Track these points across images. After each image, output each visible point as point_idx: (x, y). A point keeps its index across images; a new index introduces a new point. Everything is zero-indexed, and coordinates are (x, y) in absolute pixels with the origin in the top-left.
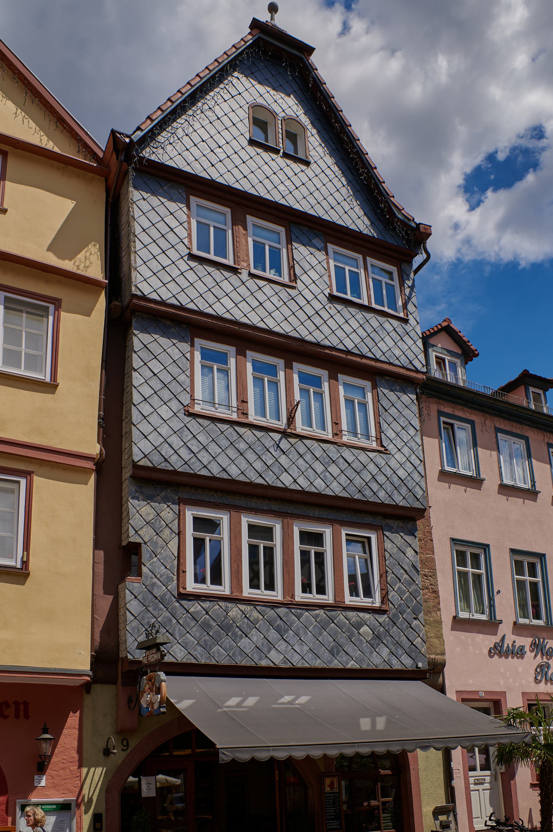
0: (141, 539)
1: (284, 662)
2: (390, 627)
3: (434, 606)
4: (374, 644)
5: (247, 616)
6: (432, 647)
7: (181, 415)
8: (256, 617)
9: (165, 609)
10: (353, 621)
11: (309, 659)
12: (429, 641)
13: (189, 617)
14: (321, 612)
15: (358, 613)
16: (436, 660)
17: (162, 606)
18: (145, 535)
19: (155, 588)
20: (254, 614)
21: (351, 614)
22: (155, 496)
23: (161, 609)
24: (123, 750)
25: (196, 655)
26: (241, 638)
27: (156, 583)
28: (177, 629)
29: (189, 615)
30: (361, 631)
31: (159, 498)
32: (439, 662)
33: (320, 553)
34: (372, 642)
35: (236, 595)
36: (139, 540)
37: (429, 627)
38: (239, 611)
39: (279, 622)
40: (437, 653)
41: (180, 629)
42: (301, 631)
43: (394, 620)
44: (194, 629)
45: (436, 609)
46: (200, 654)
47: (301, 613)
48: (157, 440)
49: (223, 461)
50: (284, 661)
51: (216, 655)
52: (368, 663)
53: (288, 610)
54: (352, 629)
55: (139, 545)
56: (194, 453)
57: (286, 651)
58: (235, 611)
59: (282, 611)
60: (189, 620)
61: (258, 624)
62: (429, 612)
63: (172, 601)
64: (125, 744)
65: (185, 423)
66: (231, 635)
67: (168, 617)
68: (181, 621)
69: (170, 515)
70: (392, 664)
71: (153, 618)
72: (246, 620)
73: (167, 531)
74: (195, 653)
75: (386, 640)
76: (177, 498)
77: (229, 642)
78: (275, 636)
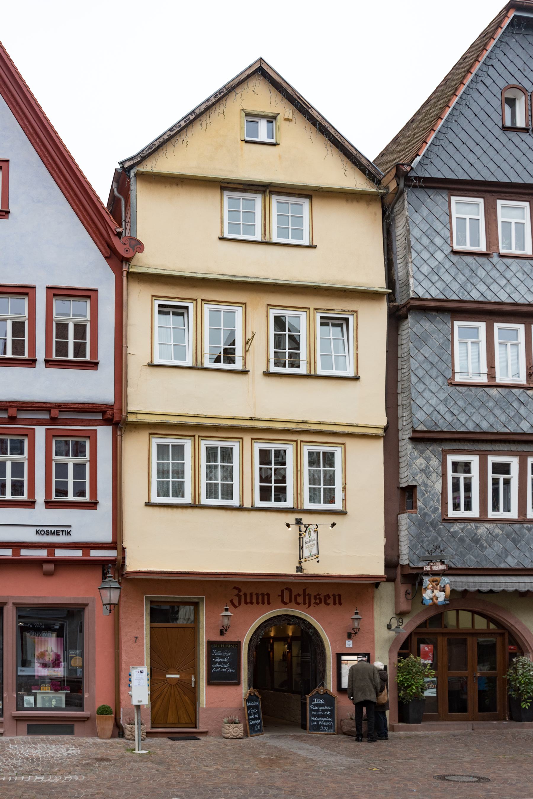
0: (416, 483)
1: (518, 565)
5: (491, 532)
7: (445, 387)
8: (497, 532)
9: (433, 531)
17: (431, 529)
18: (419, 480)
19: (427, 516)
22: (425, 450)
23: (431, 531)
25: (455, 561)
26: (486, 548)
27: (427, 513)
28: (442, 544)
29: (450, 534)
31: (428, 451)
35: (483, 518)
36: (414, 483)
38: (485, 529)
39: (514, 535)
41: (443, 544)
44: (453, 544)
48: (428, 409)
49: (476, 418)
50: (518, 564)
53: (521, 526)
55: (415, 487)
56: (455, 415)
57: (519, 556)
58: (482, 529)
59: (517, 526)
60: (449, 537)
61: (499, 538)
65: (449, 393)
66: (480, 546)
67: (435, 536)
68: (444, 539)
69: (436, 463)
72: (490, 536)
73: (434, 475)
76: (441, 449)
77: (478, 552)
78: (511, 546)
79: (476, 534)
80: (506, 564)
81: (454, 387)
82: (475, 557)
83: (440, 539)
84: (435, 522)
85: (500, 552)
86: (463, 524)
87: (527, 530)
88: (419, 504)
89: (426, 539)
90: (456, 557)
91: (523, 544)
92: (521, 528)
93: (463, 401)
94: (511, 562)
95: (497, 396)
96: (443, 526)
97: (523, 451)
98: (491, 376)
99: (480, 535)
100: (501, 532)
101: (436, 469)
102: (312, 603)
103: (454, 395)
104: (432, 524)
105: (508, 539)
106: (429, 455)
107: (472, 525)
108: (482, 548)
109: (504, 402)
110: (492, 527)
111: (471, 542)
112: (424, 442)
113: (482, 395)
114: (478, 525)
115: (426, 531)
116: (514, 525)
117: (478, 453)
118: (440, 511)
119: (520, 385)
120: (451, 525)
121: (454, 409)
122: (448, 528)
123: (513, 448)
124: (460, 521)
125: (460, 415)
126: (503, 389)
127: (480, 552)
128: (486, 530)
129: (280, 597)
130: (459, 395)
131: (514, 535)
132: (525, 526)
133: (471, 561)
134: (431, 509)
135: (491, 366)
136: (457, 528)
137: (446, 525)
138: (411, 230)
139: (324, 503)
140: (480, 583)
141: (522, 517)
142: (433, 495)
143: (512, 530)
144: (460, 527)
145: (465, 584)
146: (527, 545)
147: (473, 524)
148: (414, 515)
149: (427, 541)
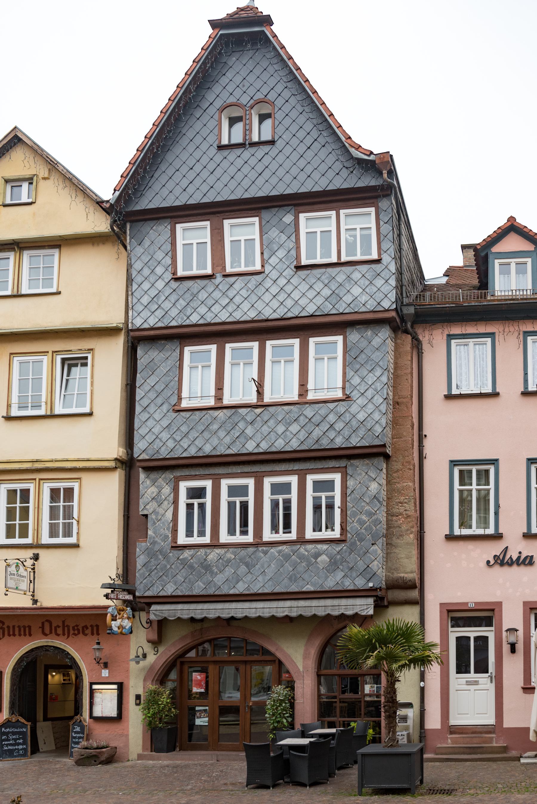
2: (347, 554)
3: (408, 530)
4: (330, 569)
5: (222, 557)
6: (401, 567)
8: (229, 557)
10: (312, 552)
11: (269, 586)
12: (400, 562)
13: (179, 563)
14: (283, 548)
15: (317, 545)
16: (405, 578)
17: (160, 557)
19: (156, 544)
20: (228, 556)
21: (310, 547)
23: (160, 559)
24: (154, 654)
26: (216, 574)
27: (157, 541)
28: (170, 572)
29: (179, 561)
30: (319, 559)
32: (407, 580)
33: (283, 501)
34: (328, 568)
37: (400, 549)
40: (406, 571)
41: (172, 572)
42: (265, 565)
43: (351, 548)
44: (182, 571)
45: (409, 532)
46: (185, 588)
47: (266, 550)
51: (197, 588)
52: (323, 586)
53: (256, 549)
54: (310, 559)
58: (213, 555)
59: (251, 550)
60: (178, 565)
62: (401, 535)
63: (167, 552)
64: (156, 650)
66: (209, 572)
70: (344, 586)
71: (154, 566)
74: (181, 588)
75: (342, 565)
77: (207, 578)
78: (244, 570)
79: (206, 560)
80: (236, 589)
81: (178, 413)
82: (204, 584)
83: (168, 567)
84: (164, 550)
85: (231, 577)
86: (192, 550)
87: (262, 553)
88: (150, 532)
89: (154, 567)
90: (184, 584)
91: (257, 569)
92: (255, 551)
93: (186, 427)
94: (241, 588)
95: (222, 418)
96: (173, 553)
97: (259, 472)
98: (219, 397)
99: (211, 561)
100: (234, 557)
101: (168, 496)
102: (71, 634)
103: (178, 421)
104: (160, 551)
105: (241, 564)
106: (161, 483)
107: (201, 551)
108: (212, 573)
109: (229, 423)
110: (223, 552)
111: (201, 569)
112: (156, 470)
113: (207, 418)
114: (208, 551)
115: (155, 560)
116: (248, 549)
117: (210, 477)
118: (170, 538)
119: (250, 403)
120: (181, 552)
121: (177, 435)
122: (177, 555)
123: (247, 469)
124: (189, 548)
125: (183, 441)
126: (229, 410)
127: (209, 578)
128: (217, 555)
129: (41, 629)
130: (183, 421)
131: (248, 559)
132: (260, 549)
133: (199, 588)
134: (161, 537)
135: (219, 388)
136: (186, 555)
137: (176, 552)
138: (132, 263)
139: (62, 537)
140: (207, 610)
141: (257, 540)
142: (163, 523)
143: (246, 554)
144: (189, 553)
145: (192, 612)
146: (261, 569)
147: (202, 551)
148: (143, 544)
149: (157, 569)
